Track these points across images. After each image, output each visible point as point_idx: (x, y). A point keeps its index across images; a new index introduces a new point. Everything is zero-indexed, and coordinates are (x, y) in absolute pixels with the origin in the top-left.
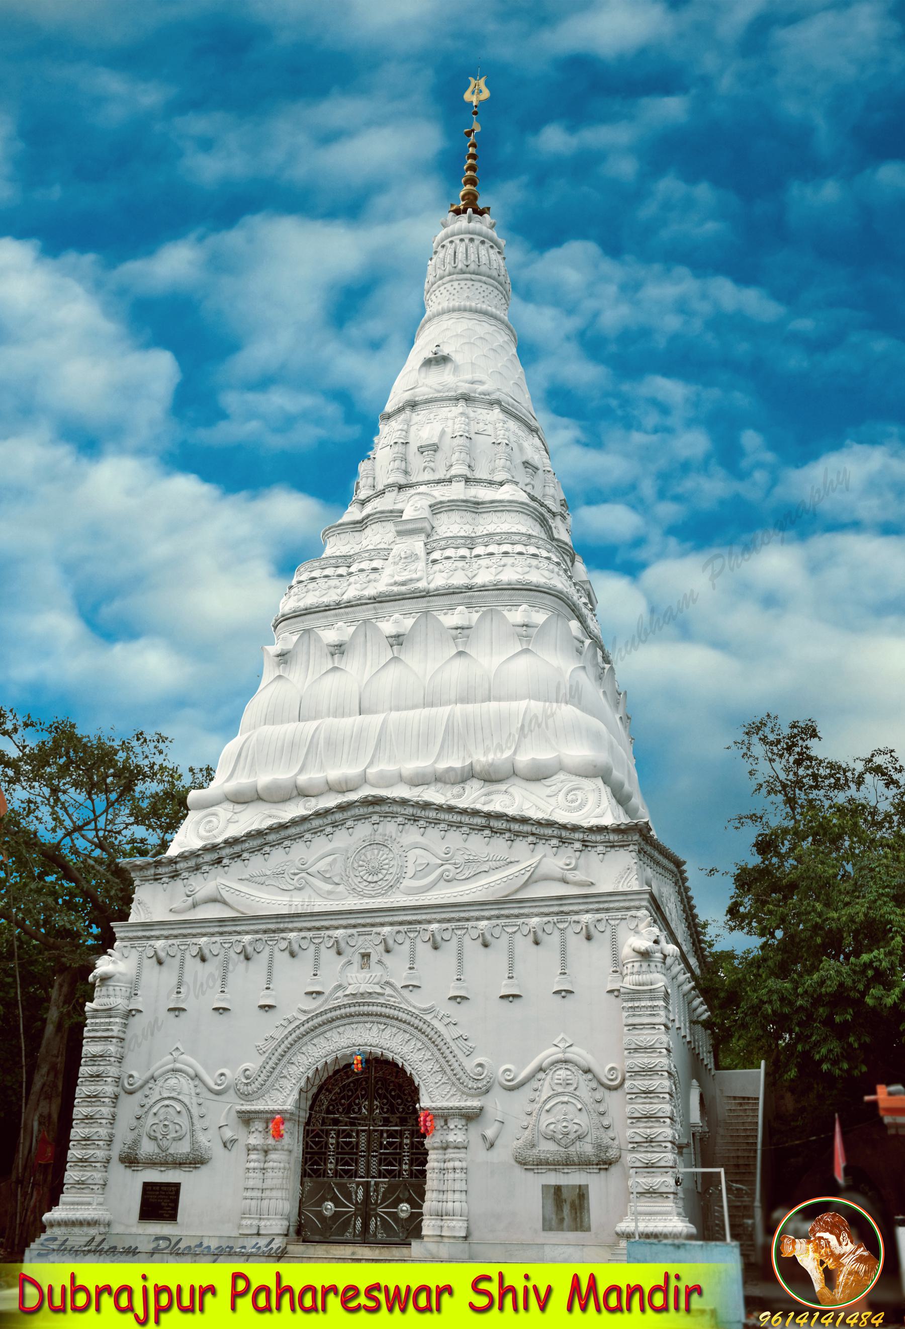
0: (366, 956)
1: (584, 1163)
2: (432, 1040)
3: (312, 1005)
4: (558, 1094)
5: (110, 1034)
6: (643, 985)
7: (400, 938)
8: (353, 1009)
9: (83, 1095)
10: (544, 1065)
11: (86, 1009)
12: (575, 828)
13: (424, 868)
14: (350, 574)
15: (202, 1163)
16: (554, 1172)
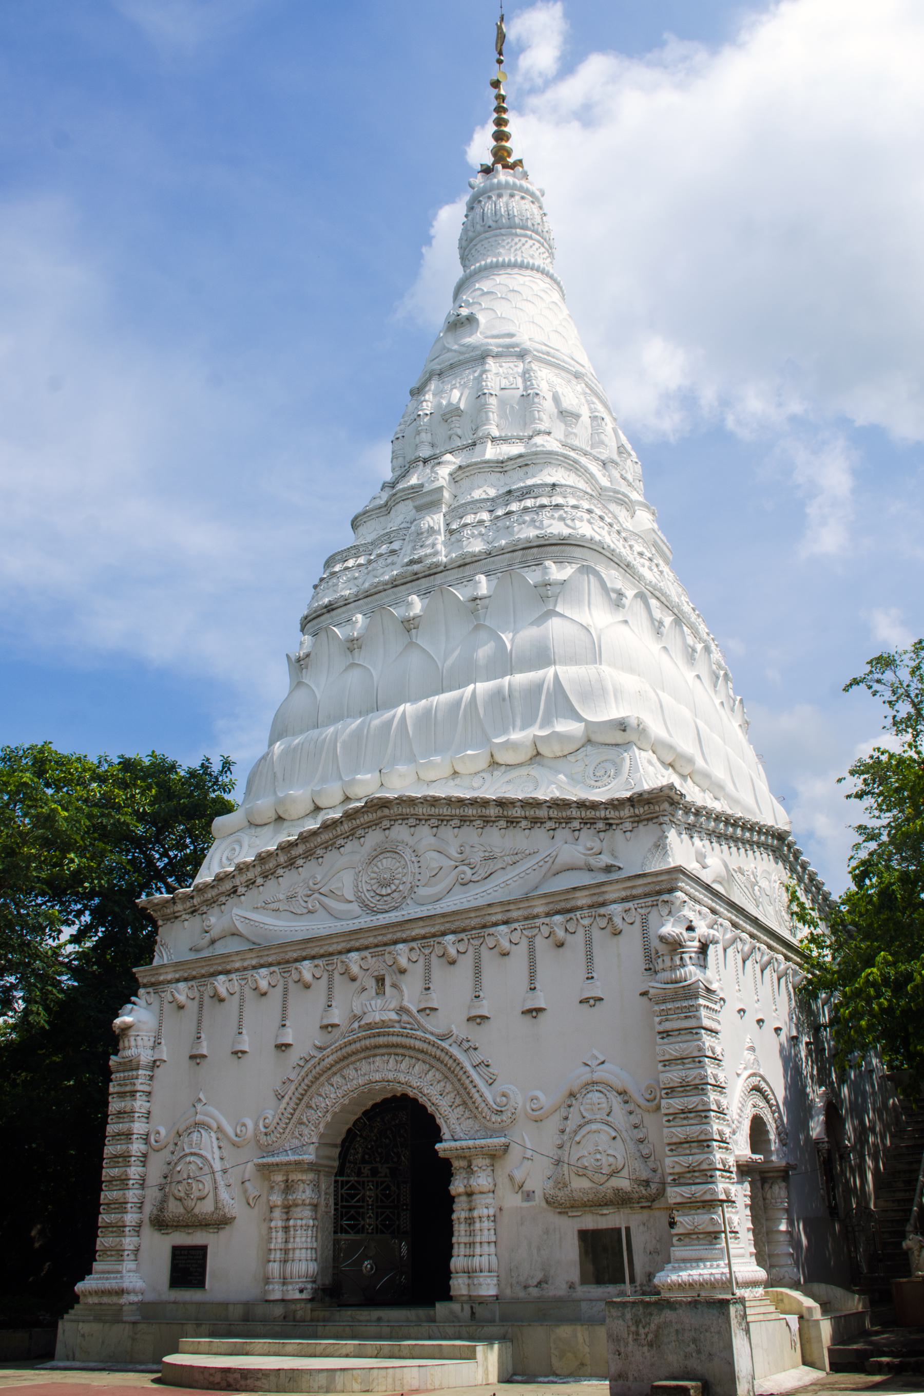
0: (380, 981)
2: (452, 1072)
4: (589, 1122)
10: (575, 1089)
11: (111, 1063)
15: (226, 1224)
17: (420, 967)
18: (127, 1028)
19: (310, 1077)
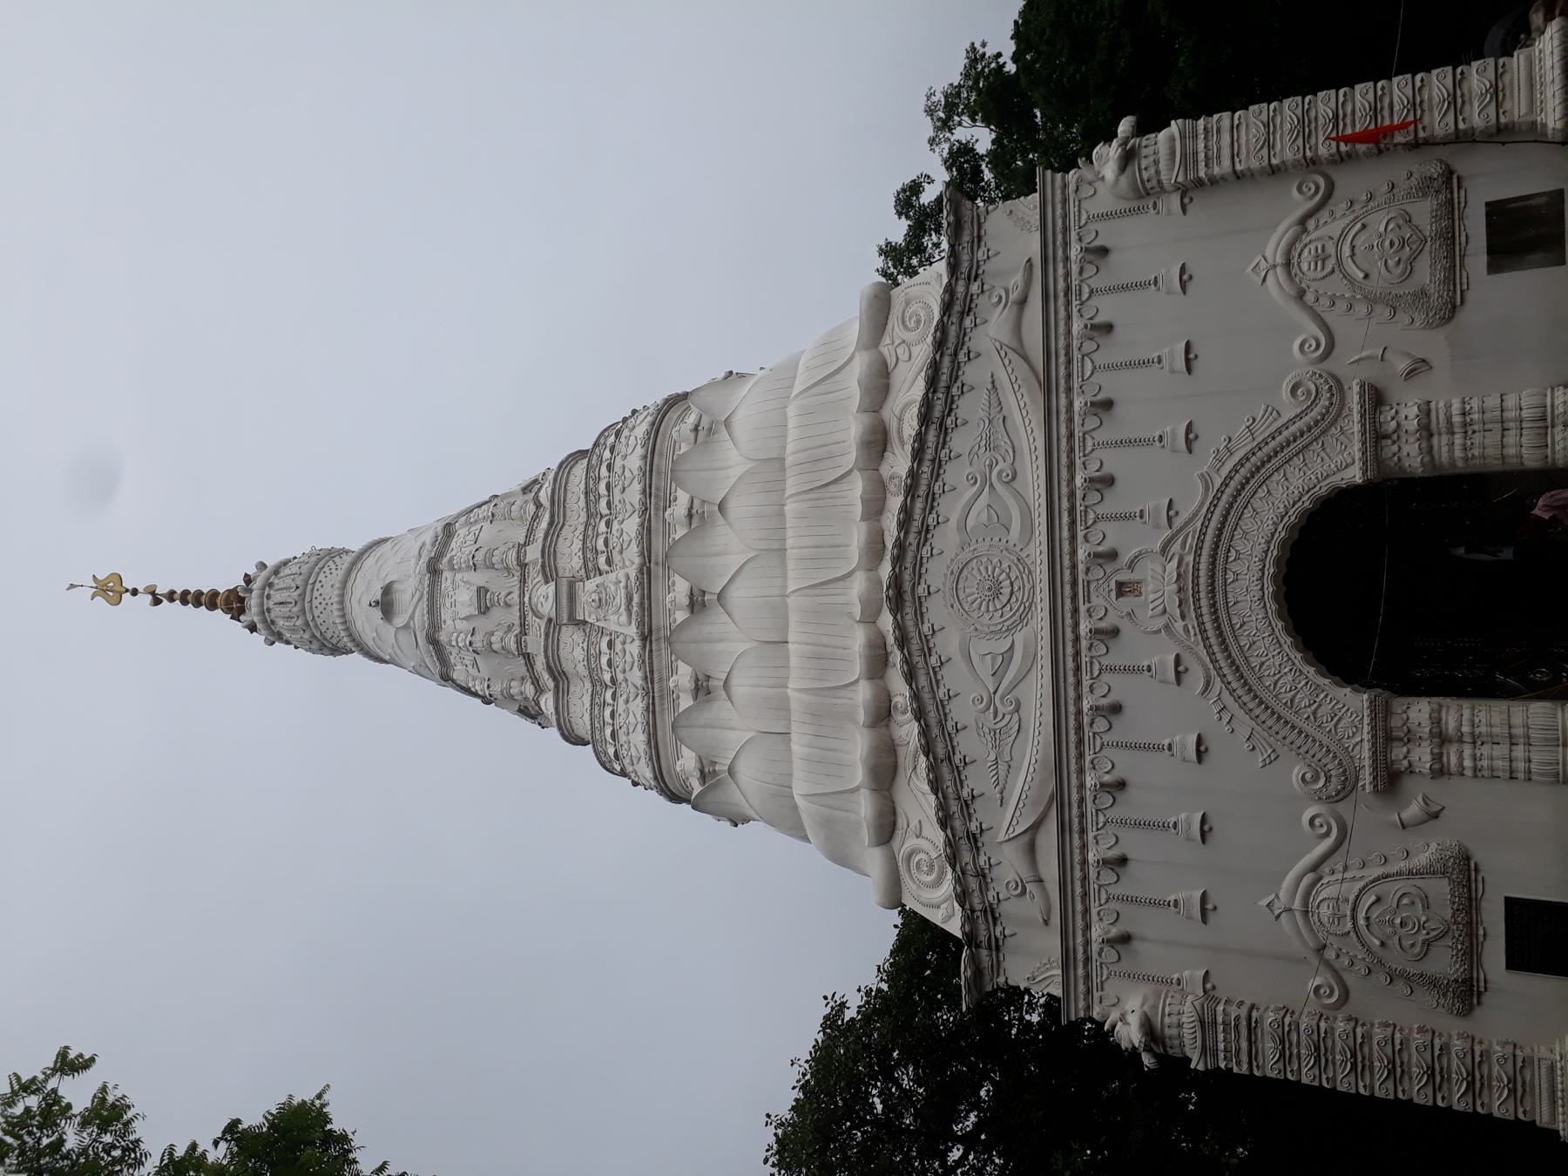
1: (1450, 211)
3: (1196, 679)
4: (1339, 262)
5: (1244, 1023)
6: (1173, 153)
8: (1204, 602)
9: (1352, 1078)
10: (1293, 292)
11: (1201, 1067)
13: (995, 504)
14: (613, 681)
15: (1468, 859)
16: (1467, 260)
17: (1110, 528)
18: (1150, 1030)
19: (1246, 699)
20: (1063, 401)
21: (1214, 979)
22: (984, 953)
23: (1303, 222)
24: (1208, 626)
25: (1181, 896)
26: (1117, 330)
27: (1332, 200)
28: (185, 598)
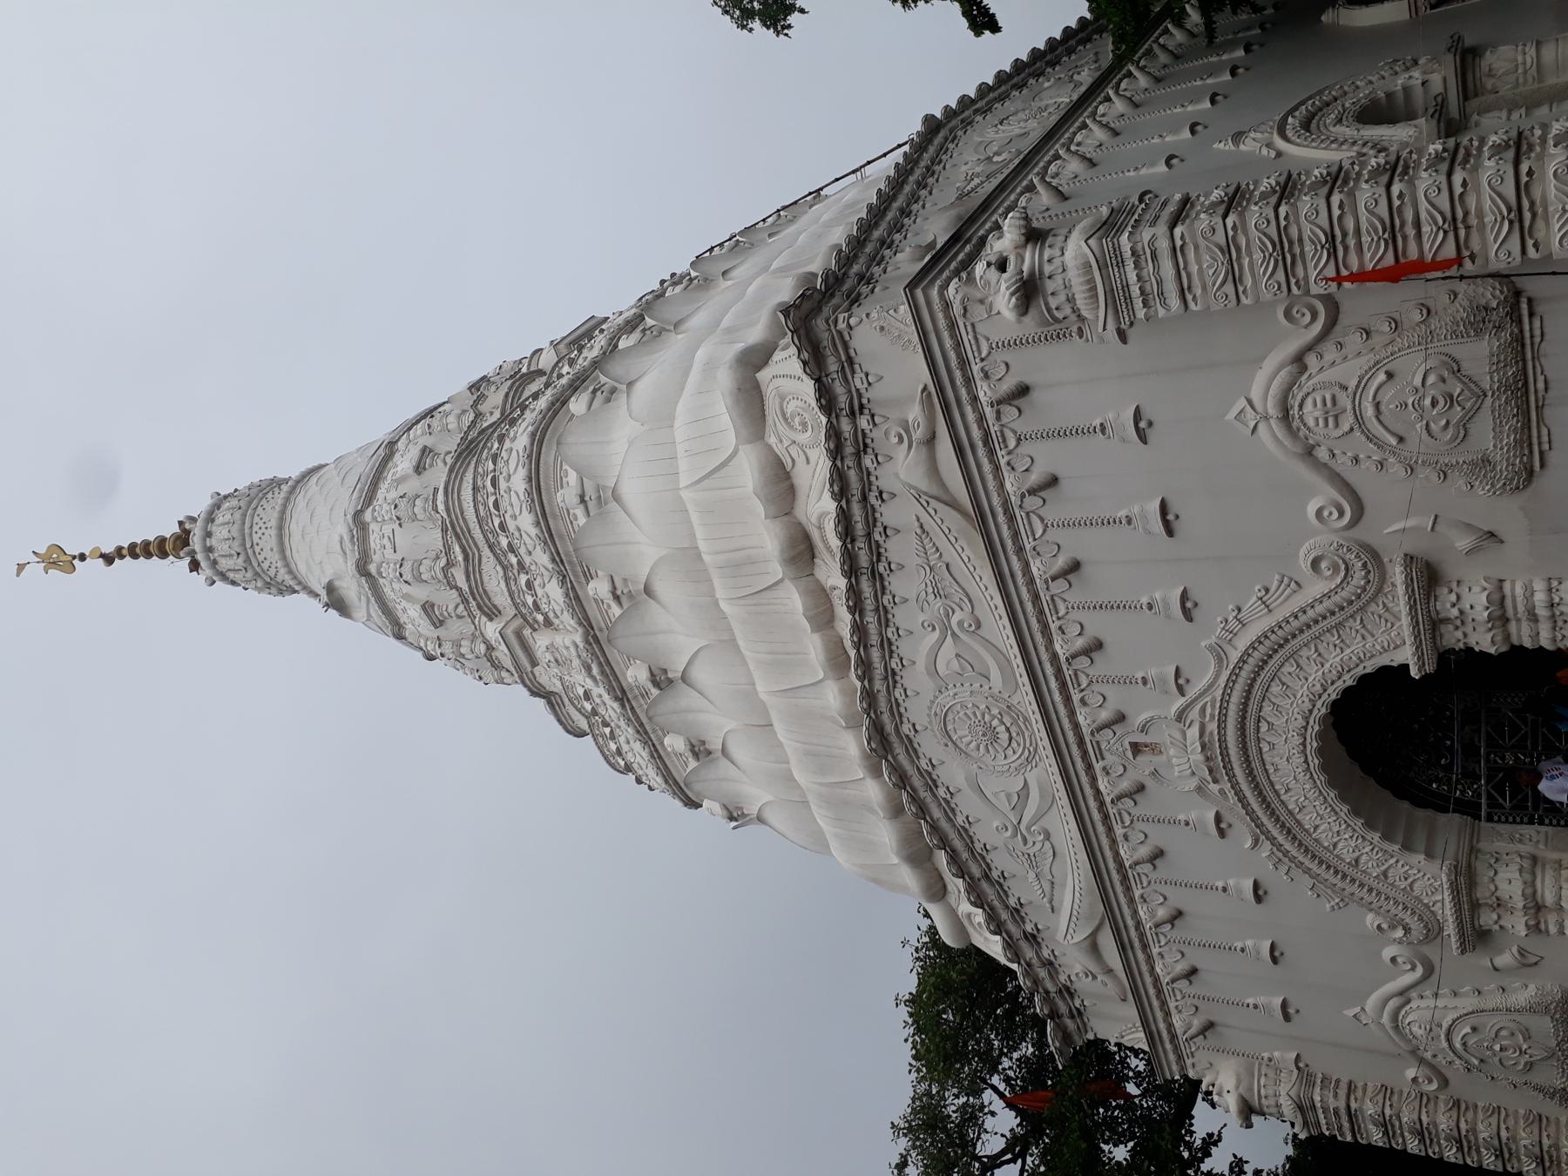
0: (1136, 748)
2: (1277, 647)
4: (1359, 419)
5: (1343, 1112)
7: (1095, 700)
10: (1299, 449)
12: (834, 434)
16: (1547, 412)
20: (1016, 565)
21: (1306, 1058)
22: (1068, 1022)
23: (1299, 360)
24: (1248, 793)
25: (1261, 1000)
26: (1063, 483)
27: (1338, 328)
28: (134, 551)
